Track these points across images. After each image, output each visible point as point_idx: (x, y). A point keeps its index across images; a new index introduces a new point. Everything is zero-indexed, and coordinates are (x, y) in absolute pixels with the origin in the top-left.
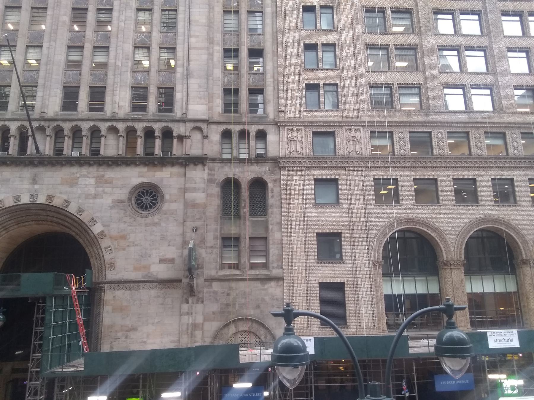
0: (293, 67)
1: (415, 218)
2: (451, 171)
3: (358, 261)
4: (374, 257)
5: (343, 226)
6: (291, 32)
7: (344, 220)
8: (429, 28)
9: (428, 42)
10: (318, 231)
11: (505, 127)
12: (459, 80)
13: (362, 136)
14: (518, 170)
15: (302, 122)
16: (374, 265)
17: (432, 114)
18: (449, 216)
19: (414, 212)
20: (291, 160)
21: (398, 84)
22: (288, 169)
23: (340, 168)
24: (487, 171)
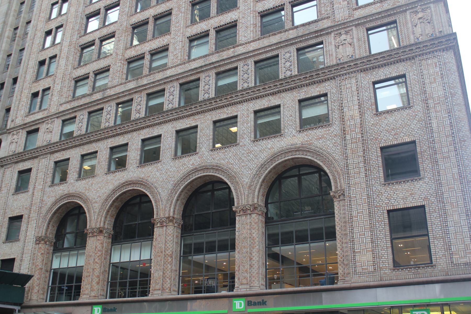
0: (27, 83)
1: (74, 192)
2: (110, 140)
3: (27, 238)
4: (38, 233)
5: (26, 208)
6: (33, 56)
7: (27, 204)
9: (121, 25)
10: (10, 216)
11: (165, 83)
13: (55, 126)
15: (20, 126)
16: (36, 240)
17: (108, 90)
18: (99, 185)
19: (74, 186)
20: (5, 159)
22: (5, 167)
23: (35, 158)
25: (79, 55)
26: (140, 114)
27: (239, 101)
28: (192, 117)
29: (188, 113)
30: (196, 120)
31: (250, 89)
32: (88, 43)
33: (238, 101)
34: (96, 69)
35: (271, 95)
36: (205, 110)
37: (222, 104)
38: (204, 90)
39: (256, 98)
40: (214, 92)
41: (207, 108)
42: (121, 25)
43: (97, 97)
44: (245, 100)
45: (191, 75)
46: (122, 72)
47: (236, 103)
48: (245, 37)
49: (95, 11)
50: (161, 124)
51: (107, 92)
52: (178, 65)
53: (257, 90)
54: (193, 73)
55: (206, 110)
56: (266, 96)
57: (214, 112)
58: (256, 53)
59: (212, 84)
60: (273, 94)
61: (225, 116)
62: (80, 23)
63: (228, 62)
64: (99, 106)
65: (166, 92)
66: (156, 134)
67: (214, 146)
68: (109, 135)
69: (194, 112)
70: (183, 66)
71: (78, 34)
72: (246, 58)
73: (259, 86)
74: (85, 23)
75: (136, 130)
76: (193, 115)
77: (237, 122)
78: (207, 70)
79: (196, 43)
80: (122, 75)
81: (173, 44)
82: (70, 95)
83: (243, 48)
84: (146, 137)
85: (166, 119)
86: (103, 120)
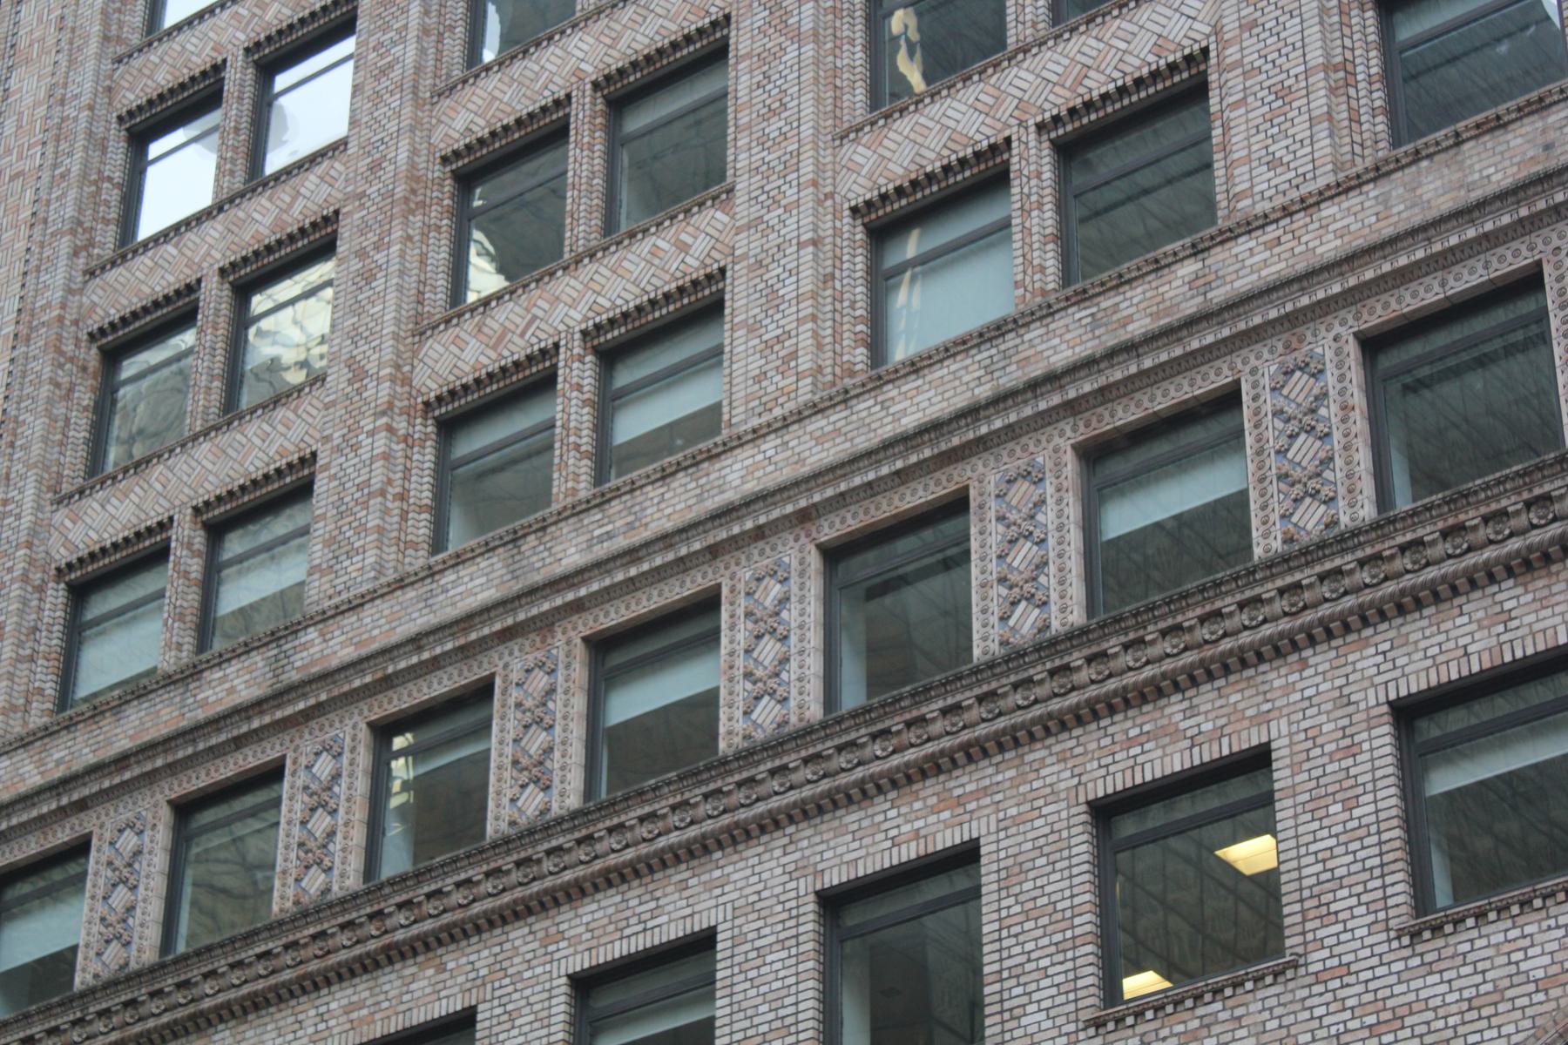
8: (396, 74)
9: (375, 167)
11: (714, 551)
12: (522, 335)
14: (751, 852)
17: (312, 634)
21: (196, 510)
24: (553, 930)
25: (85, 396)
26: (547, 788)
27: (1269, 640)
28: (930, 789)
29: (896, 760)
30: (960, 801)
31: (1344, 540)
32: (146, 310)
33: (1263, 642)
34: (211, 487)
35: (1510, 572)
36: (1023, 726)
37: (1148, 672)
38: (1002, 580)
39: (1401, 610)
40: (1077, 590)
41: (1037, 711)
42: (375, 167)
43: (231, 691)
44: (1318, 631)
45: (902, 476)
46: (402, 497)
47: (1250, 656)
48: (1273, 164)
49: (183, 86)
50: (707, 850)
51: (305, 647)
52: (799, 417)
53: (1403, 548)
54: (913, 459)
55: (1034, 722)
56: (1473, 585)
57: (1090, 739)
58: (1369, 275)
59: (1060, 528)
60: (1528, 565)
61: (1176, 761)
62: (84, 175)
63: (1164, 357)
64: (248, 751)
65: (724, 615)
66: (674, 932)
67: (1111, 991)
68: (333, 960)
69: (946, 743)
70: (837, 416)
71: (76, 253)
72: (1293, 320)
73: (1414, 513)
74: (118, 176)
75: (530, 912)
76: (939, 770)
77: (1266, 801)
78: (1011, 433)
79: (912, 245)
80: (404, 516)
81: (750, 269)
82: (41, 691)
83: (1269, 246)
84: (605, 955)
85: (742, 815)
86: (286, 857)
